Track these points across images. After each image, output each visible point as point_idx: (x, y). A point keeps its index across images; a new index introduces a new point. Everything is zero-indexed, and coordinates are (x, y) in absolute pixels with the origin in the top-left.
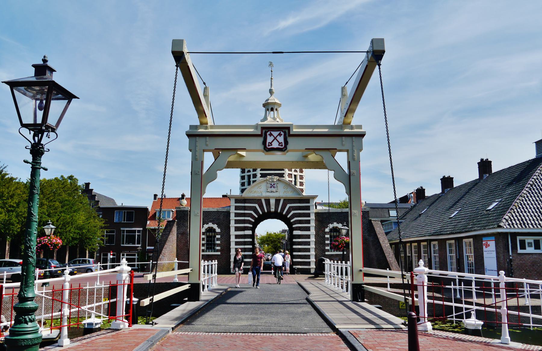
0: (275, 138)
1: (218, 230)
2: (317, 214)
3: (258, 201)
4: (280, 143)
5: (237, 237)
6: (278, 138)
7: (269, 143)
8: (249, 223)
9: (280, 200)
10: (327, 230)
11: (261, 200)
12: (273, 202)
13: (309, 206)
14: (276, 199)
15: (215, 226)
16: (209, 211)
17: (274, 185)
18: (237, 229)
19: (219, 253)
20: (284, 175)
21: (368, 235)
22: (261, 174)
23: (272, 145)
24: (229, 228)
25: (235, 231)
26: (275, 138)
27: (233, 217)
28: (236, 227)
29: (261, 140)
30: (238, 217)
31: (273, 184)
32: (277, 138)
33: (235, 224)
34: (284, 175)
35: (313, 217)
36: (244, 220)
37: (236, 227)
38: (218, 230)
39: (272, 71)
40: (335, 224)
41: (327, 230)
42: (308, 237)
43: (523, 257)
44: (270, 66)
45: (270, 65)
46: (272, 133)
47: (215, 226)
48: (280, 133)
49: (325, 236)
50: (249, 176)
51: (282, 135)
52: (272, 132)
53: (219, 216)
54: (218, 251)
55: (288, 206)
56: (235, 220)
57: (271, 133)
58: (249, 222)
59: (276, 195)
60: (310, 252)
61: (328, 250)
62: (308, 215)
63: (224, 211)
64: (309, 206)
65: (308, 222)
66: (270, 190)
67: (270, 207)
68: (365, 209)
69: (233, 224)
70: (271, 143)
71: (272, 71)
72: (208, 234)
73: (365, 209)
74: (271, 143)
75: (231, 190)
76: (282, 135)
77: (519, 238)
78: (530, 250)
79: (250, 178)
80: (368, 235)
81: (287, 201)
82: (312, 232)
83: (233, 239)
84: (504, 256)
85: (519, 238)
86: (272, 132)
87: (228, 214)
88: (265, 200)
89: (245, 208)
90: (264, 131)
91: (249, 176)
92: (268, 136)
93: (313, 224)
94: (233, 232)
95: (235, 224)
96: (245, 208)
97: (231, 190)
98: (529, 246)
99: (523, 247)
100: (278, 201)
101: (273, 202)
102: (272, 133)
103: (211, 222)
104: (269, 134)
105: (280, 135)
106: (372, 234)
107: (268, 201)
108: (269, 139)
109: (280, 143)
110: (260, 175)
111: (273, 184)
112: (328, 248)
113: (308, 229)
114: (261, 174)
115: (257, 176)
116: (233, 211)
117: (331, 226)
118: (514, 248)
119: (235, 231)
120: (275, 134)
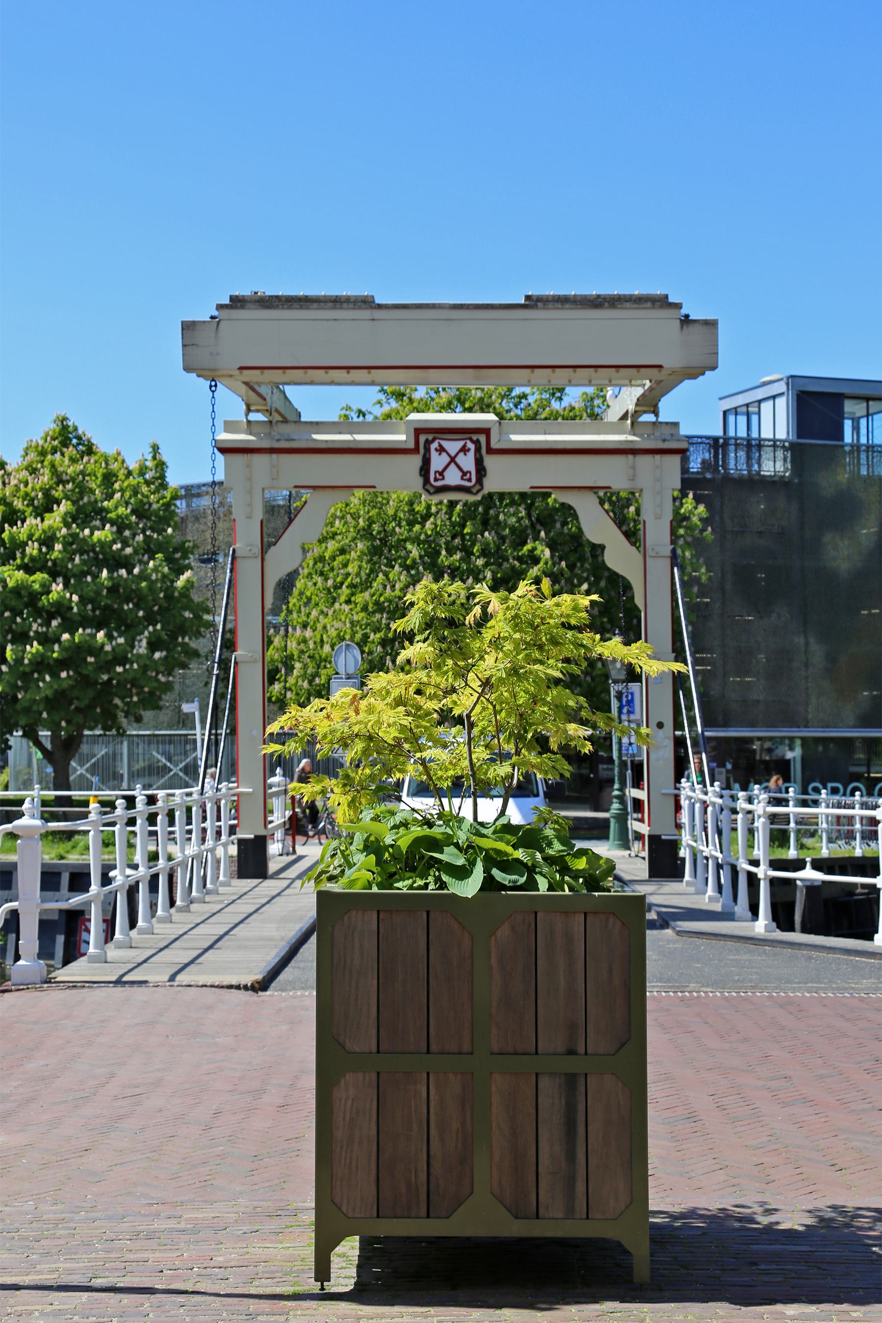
0: (453, 460)
4: (464, 474)
6: (460, 459)
7: (436, 472)
23: (443, 478)
26: (453, 460)
29: (416, 461)
32: (457, 460)
46: (445, 444)
48: (465, 446)
51: (469, 450)
52: (443, 443)
57: (440, 445)
70: (441, 473)
74: (441, 473)
75: (721, 399)
76: (469, 450)
86: (443, 443)
90: (422, 438)
92: (434, 455)
97: (721, 399)
102: (445, 444)
104: (436, 450)
105: (464, 450)
108: (438, 462)
109: (464, 474)
120: (453, 447)
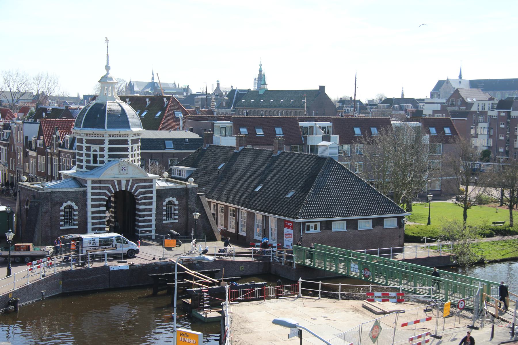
1: (76, 207)
2: (158, 191)
3: (112, 182)
5: (93, 213)
8: (104, 201)
9: (129, 180)
10: (165, 203)
11: (114, 181)
12: (124, 183)
13: (152, 185)
14: (126, 180)
15: (73, 204)
16: (67, 191)
17: (125, 168)
18: (93, 206)
19: (77, 227)
20: (128, 156)
21: (196, 207)
22: (108, 155)
24: (86, 205)
25: (92, 207)
27: (89, 196)
28: (92, 205)
30: (94, 196)
31: (124, 167)
33: (92, 202)
34: (128, 156)
35: (154, 195)
36: (100, 198)
37: (92, 205)
38: (76, 207)
39: (107, 47)
40: (171, 199)
41: (165, 203)
42: (151, 210)
43: (307, 235)
44: (106, 42)
45: (106, 41)
47: (73, 204)
49: (162, 208)
50: (95, 156)
53: (76, 195)
54: (75, 225)
55: (136, 185)
56: (92, 198)
58: (104, 200)
59: (127, 177)
60: (151, 222)
61: (165, 219)
62: (151, 192)
63: (80, 191)
64: (152, 185)
65: (151, 198)
66: (122, 172)
67: (121, 186)
68: (195, 186)
69: (89, 202)
71: (107, 47)
72: (66, 210)
73: (195, 186)
77: (307, 224)
78: (312, 231)
79: (97, 157)
80: (196, 207)
81: (135, 181)
82: (154, 206)
83: (90, 215)
84: (298, 235)
85: (307, 224)
87: (85, 193)
88: (117, 180)
89: (100, 188)
91: (95, 156)
93: (154, 200)
94: (90, 209)
95: (92, 202)
96: (100, 188)
98: (311, 228)
99: (308, 229)
100: (128, 181)
101: (124, 183)
103: (69, 200)
106: (199, 206)
107: (119, 182)
110: (108, 156)
111: (124, 167)
112: (164, 218)
113: (151, 204)
114: (108, 155)
115: (104, 156)
116: (89, 191)
117: (167, 200)
118: (304, 230)
119: (92, 207)
